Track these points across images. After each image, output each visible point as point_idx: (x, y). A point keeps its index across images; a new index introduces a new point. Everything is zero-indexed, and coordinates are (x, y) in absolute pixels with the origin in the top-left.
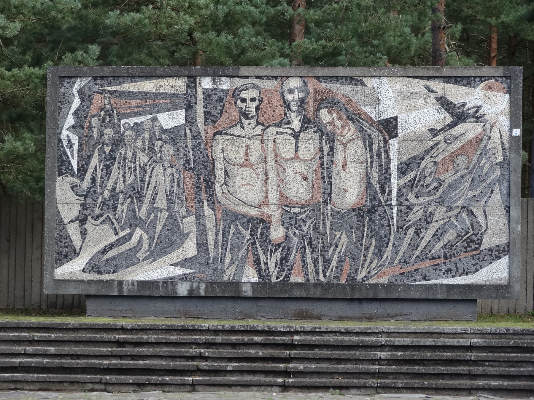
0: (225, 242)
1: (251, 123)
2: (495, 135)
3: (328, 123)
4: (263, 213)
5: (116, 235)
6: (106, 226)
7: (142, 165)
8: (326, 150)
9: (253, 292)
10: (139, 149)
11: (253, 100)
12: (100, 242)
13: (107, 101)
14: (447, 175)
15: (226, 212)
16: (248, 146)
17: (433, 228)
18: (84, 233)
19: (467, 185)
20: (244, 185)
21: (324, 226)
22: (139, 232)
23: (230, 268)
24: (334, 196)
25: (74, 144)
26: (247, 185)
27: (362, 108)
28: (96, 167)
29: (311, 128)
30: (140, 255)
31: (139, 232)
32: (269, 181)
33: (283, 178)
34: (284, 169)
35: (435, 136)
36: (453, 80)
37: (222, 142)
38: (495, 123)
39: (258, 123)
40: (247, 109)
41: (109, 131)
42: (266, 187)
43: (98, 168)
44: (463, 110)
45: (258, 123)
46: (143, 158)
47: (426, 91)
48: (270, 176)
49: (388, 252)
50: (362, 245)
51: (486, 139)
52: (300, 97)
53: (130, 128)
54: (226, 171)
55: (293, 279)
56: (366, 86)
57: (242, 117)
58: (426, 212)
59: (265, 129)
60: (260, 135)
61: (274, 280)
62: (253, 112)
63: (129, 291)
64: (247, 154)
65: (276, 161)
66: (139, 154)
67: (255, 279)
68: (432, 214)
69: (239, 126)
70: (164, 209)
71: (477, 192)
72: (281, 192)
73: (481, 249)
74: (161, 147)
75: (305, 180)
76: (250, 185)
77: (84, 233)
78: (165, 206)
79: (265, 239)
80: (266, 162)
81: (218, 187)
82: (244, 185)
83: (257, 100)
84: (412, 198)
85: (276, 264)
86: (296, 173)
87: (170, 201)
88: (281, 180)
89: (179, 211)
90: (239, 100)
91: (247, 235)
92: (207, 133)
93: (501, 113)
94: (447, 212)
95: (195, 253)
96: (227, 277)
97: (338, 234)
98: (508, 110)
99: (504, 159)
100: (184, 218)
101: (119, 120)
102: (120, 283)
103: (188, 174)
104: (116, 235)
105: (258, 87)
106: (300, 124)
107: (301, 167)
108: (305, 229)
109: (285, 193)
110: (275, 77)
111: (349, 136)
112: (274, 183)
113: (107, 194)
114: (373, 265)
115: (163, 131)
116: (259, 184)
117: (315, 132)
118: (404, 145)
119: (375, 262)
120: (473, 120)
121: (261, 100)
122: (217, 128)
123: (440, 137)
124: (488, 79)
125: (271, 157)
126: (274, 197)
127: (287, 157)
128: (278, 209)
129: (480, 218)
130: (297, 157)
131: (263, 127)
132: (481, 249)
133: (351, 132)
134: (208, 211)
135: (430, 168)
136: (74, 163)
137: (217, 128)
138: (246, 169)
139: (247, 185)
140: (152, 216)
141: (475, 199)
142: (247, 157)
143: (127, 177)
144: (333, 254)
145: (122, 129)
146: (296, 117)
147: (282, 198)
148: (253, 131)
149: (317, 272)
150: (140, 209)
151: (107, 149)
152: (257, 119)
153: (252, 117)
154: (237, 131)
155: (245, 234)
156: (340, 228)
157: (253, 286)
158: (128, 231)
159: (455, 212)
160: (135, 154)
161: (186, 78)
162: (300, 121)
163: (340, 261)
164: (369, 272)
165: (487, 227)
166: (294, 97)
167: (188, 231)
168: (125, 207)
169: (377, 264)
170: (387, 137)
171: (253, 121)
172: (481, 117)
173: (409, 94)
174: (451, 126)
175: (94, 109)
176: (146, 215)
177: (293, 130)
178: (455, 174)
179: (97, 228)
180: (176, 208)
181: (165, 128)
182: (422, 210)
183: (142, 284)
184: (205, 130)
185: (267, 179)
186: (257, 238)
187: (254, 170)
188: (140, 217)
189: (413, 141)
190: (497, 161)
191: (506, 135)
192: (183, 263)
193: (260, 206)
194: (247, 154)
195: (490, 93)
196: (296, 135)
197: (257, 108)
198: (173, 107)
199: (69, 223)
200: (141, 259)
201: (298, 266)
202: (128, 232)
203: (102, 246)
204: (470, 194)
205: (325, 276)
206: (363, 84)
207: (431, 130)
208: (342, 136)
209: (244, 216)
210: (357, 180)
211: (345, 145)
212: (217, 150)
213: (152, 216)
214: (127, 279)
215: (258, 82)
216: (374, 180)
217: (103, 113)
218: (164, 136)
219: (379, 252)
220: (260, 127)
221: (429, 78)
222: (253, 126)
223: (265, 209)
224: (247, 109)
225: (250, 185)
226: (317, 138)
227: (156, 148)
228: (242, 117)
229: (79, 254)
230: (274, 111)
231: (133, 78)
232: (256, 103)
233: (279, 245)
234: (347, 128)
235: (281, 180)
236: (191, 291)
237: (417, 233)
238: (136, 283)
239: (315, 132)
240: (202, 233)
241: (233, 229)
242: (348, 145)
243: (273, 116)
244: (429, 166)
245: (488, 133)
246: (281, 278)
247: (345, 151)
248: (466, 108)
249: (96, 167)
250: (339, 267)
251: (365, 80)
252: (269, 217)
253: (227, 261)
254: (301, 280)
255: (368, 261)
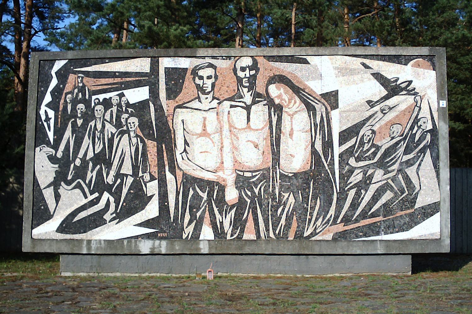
0: (184, 203)
1: (207, 98)
2: (425, 106)
3: (276, 97)
4: (219, 177)
5: (85, 198)
6: (78, 191)
7: (110, 136)
8: (275, 119)
9: (210, 248)
10: (107, 121)
11: (209, 77)
12: (71, 205)
13: (79, 80)
14: (384, 141)
15: (185, 176)
16: (205, 119)
17: (373, 189)
18: (57, 197)
19: (402, 149)
20: (201, 152)
21: (274, 188)
22: (106, 195)
23: (189, 227)
24: (282, 161)
25: (51, 118)
26: (204, 152)
27: (306, 83)
28: (69, 138)
29: (261, 101)
30: (107, 217)
31: (106, 195)
32: (224, 149)
33: (237, 145)
34: (237, 138)
35: (372, 107)
36: (387, 58)
37: (182, 114)
38: (424, 95)
39: (214, 98)
40: (204, 86)
41: (81, 106)
42: (222, 154)
43: (71, 138)
44: (396, 84)
45: (214, 98)
46: (110, 129)
47: (363, 67)
48: (224, 144)
49: (332, 212)
50: (308, 205)
51: (417, 109)
52: (251, 74)
53: (99, 103)
54: (185, 140)
55: (246, 237)
56: (309, 64)
57: (199, 93)
58: (365, 175)
59: (219, 104)
60: (216, 108)
61: (229, 237)
62: (209, 89)
63: (97, 249)
64: (204, 126)
65: (230, 131)
66: (108, 125)
67: (211, 236)
68: (371, 177)
69: (197, 100)
70: (130, 175)
71: (411, 156)
72: (234, 158)
73: (416, 208)
74: (127, 119)
75: (256, 147)
76: (207, 152)
77: (57, 197)
78: (130, 173)
79: (221, 201)
80: (221, 131)
81: (178, 153)
82: (201, 152)
83: (213, 77)
84: (352, 161)
85: (231, 222)
86: (249, 141)
87: (135, 168)
88: (235, 148)
89: (143, 176)
90: (197, 78)
91: (205, 196)
92: (169, 107)
93: (429, 87)
94: (384, 174)
95: (158, 214)
96: (186, 235)
97: (286, 195)
98: (435, 84)
99: (433, 127)
100: (147, 182)
101: (90, 97)
102: (89, 242)
103: (152, 143)
104: (85, 198)
105: (214, 67)
106: (252, 98)
107: (253, 136)
108: (256, 191)
109: (239, 159)
110: (229, 57)
111: (294, 109)
112: (229, 150)
113: (78, 162)
114: (319, 223)
115: (128, 105)
116: (215, 151)
117: (264, 105)
118: (345, 115)
119: (320, 220)
120: (405, 92)
121: (216, 77)
122: (177, 102)
123: (377, 108)
124: (417, 58)
125: (226, 127)
126: (229, 164)
127: (240, 128)
128: (232, 173)
129: (415, 181)
130: (249, 127)
131: (219, 101)
132: (416, 208)
133: (297, 104)
134: (169, 176)
135: (369, 136)
136: (51, 135)
137: (177, 102)
138: (203, 138)
139: (204, 152)
140: (119, 181)
141: (409, 163)
142: (205, 127)
143: (96, 147)
144: (282, 214)
145: (93, 104)
146: (248, 92)
147: (236, 164)
148: (209, 104)
149: (268, 230)
150: (108, 174)
151: (80, 122)
152: (213, 94)
153: (209, 92)
154: (195, 104)
155: (202, 196)
156: (288, 189)
157: (209, 245)
158: (96, 195)
159: (391, 175)
160: (103, 126)
161: (150, 59)
162: (251, 95)
163: (289, 219)
164: (316, 229)
165: (420, 188)
166: (245, 75)
167: (151, 194)
168: (95, 173)
169: (322, 222)
170: (329, 108)
171: (210, 96)
172: (412, 91)
173: (348, 70)
174: (386, 98)
175: (68, 88)
176: (113, 181)
177: (245, 103)
178: (391, 140)
179: (69, 193)
180: (141, 174)
181: (131, 103)
182: (362, 173)
183: (109, 242)
184: (167, 104)
185: (222, 147)
186: (213, 199)
187: (211, 139)
188: (107, 182)
189: (352, 111)
190: (427, 129)
191: (434, 107)
192: (146, 224)
193: (216, 171)
194: (204, 126)
195: (420, 70)
196: (248, 108)
197: (213, 85)
198: (138, 84)
199: (44, 188)
200: (108, 220)
201: (250, 224)
202: (97, 196)
203: (73, 209)
204: (406, 158)
205: (274, 234)
206: (308, 63)
207: (369, 102)
208: (289, 108)
209: (201, 180)
210: (304, 147)
211: (292, 116)
212: (177, 121)
213: (119, 181)
214: (95, 239)
215: (213, 61)
216: (319, 146)
217: (76, 91)
218: (130, 110)
219: (325, 210)
220: (216, 101)
221: (366, 56)
222: (210, 99)
223: (220, 174)
224: (204, 86)
225: (207, 152)
226: (267, 110)
227: (122, 120)
228: (199, 93)
229: (53, 215)
230: (228, 87)
231: (102, 60)
232: (213, 80)
233: (232, 207)
234: (293, 101)
235: (235, 148)
236: (153, 248)
237: (358, 194)
238: (103, 242)
239: (264, 105)
240: (163, 197)
241: (191, 192)
242: (295, 116)
243: (227, 91)
244: (367, 134)
245: (418, 105)
246: (235, 236)
247: (292, 121)
248: (399, 83)
249: (69, 138)
250: (288, 225)
251: (309, 58)
252: (224, 181)
253: (186, 220)
254: (253, 237)
255: (314, 219)
